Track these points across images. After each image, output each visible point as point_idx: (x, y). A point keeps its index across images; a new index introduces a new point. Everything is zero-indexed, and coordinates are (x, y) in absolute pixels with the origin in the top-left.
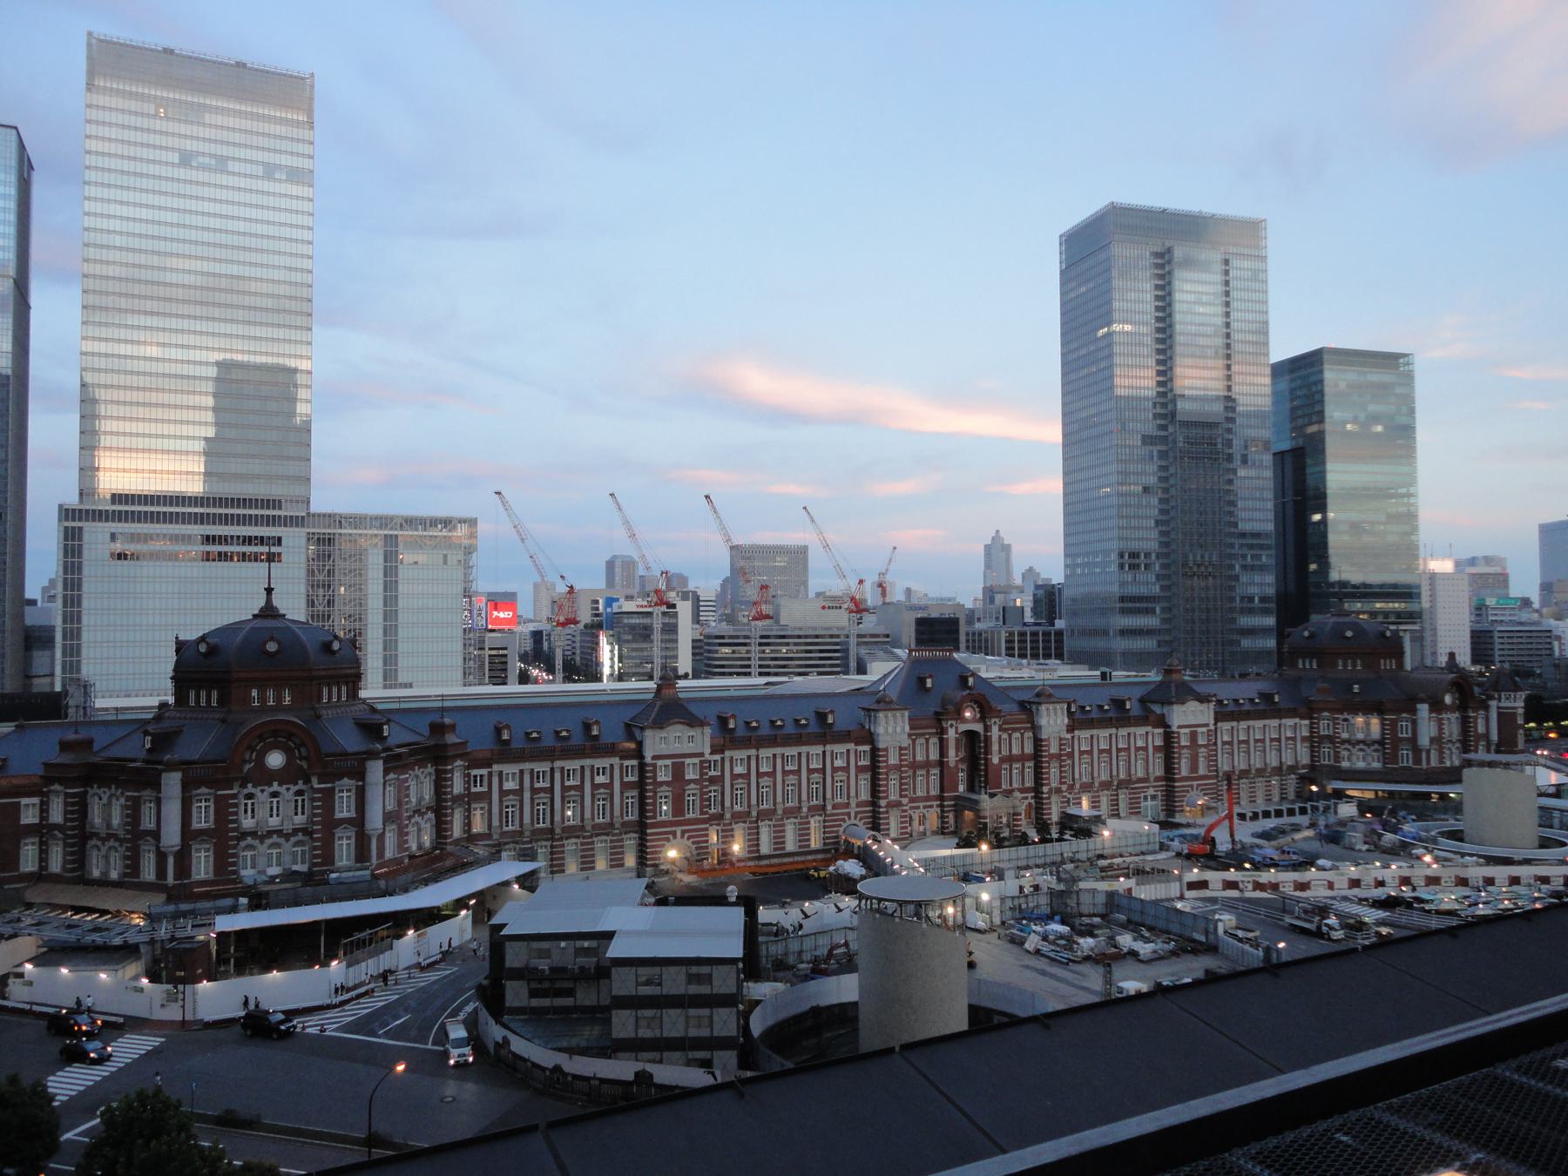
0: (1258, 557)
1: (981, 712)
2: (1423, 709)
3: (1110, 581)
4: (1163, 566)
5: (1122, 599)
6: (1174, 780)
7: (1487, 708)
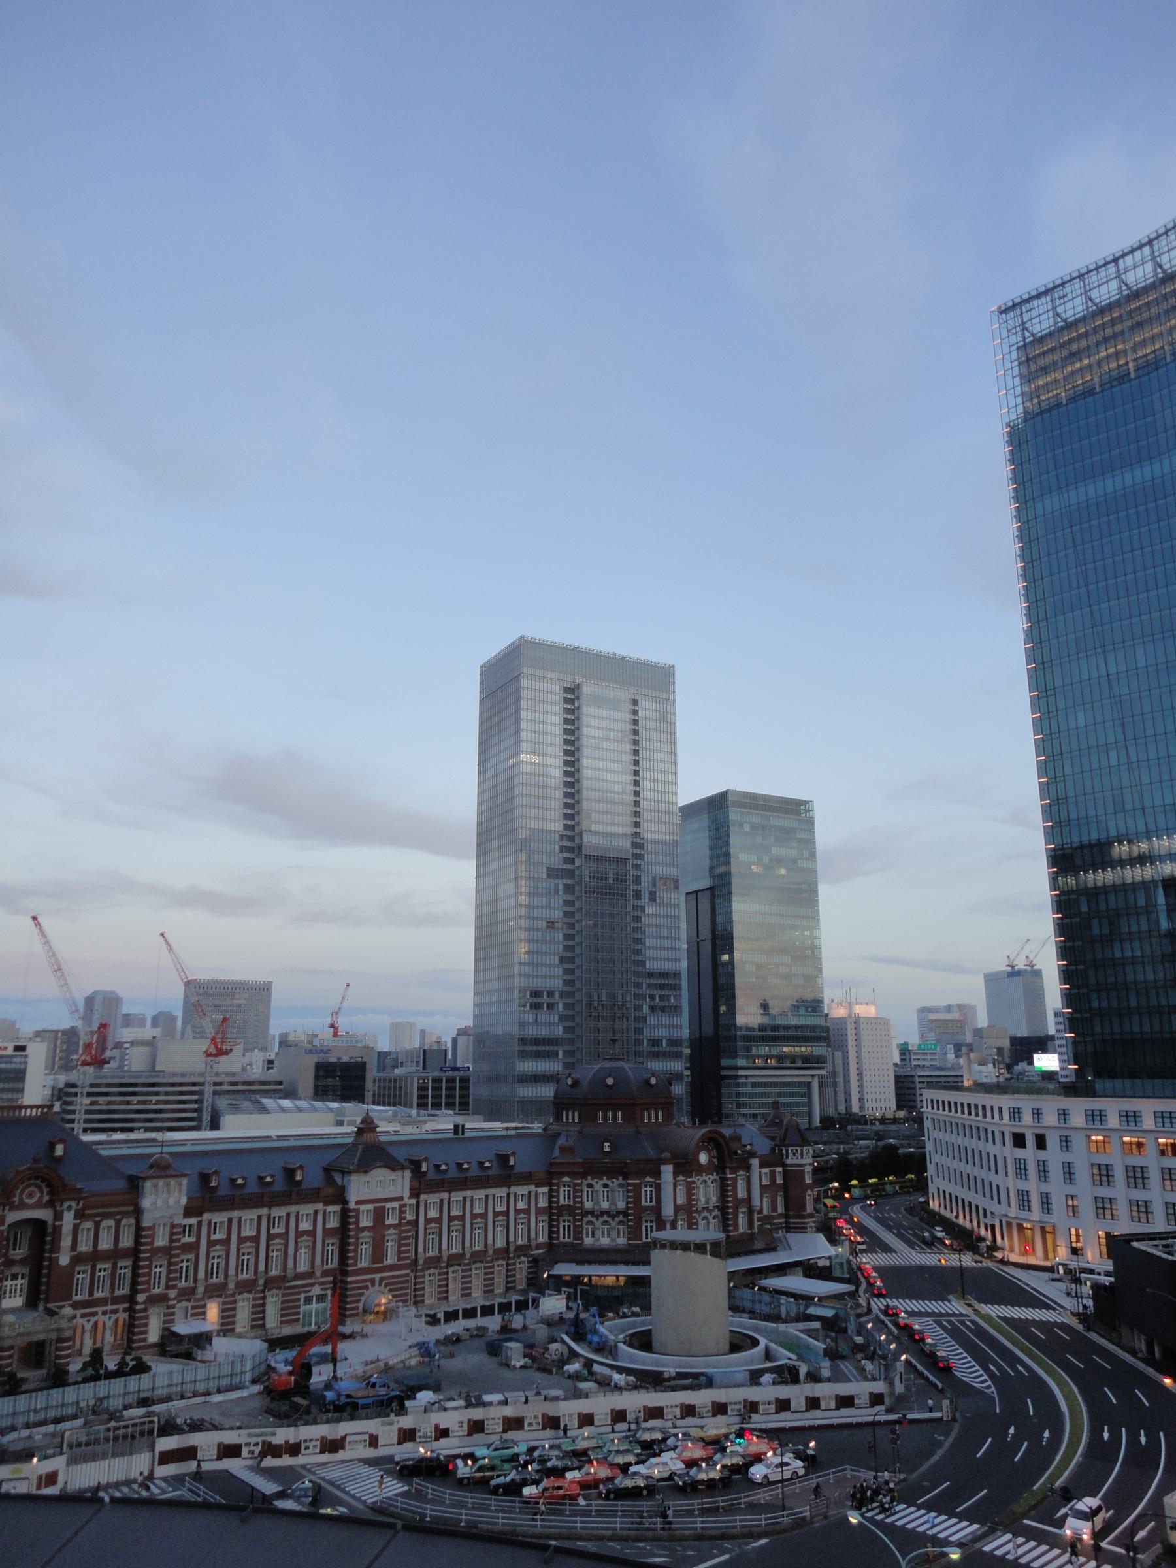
1: (51, 1193)
2: (667, 1170)
3: (513, 1020)
5: (522, 1041)
7: (748, 1168)
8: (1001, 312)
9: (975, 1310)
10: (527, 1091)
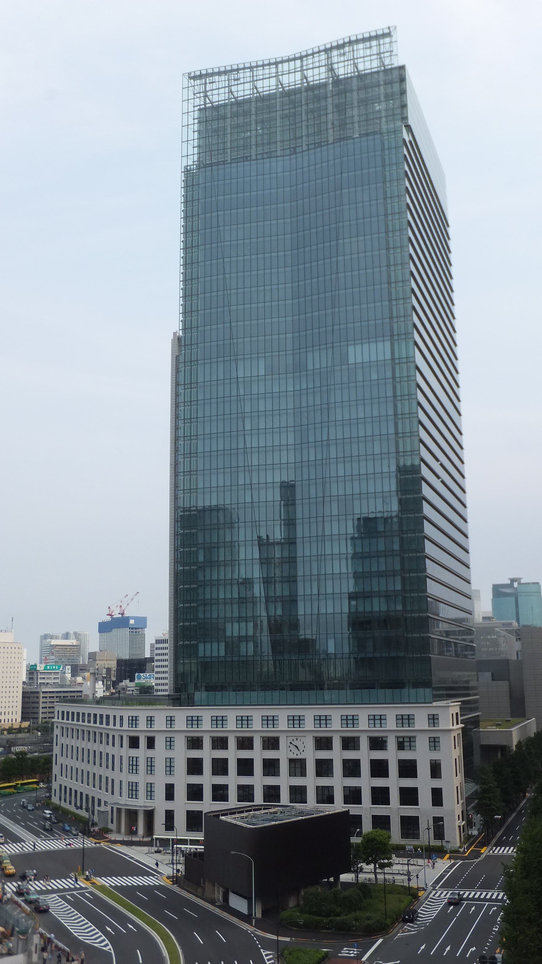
8: (190, 78)
9: (93, 883)
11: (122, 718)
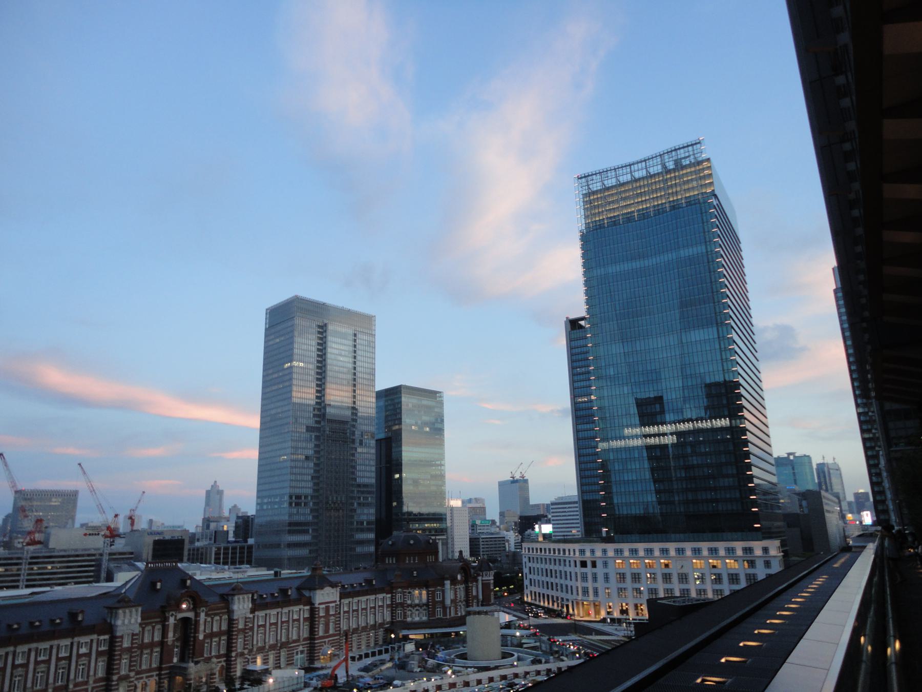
0: (367, 498)
2: (448, 583)
3: (283, 513)
4: (314, 503)
5: (290, 524)
6: (314, 639)
7: (477, 581)
10: (290, 553)
11: (574, 550)
